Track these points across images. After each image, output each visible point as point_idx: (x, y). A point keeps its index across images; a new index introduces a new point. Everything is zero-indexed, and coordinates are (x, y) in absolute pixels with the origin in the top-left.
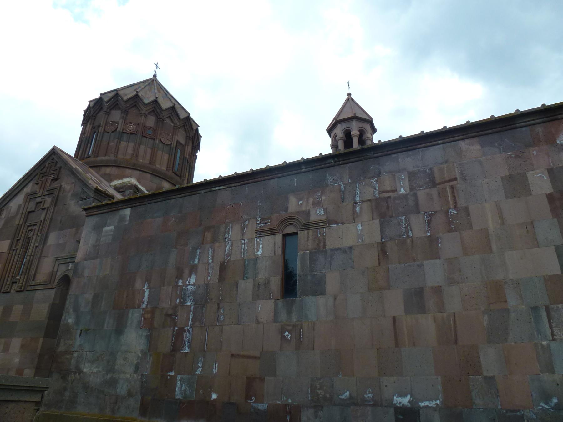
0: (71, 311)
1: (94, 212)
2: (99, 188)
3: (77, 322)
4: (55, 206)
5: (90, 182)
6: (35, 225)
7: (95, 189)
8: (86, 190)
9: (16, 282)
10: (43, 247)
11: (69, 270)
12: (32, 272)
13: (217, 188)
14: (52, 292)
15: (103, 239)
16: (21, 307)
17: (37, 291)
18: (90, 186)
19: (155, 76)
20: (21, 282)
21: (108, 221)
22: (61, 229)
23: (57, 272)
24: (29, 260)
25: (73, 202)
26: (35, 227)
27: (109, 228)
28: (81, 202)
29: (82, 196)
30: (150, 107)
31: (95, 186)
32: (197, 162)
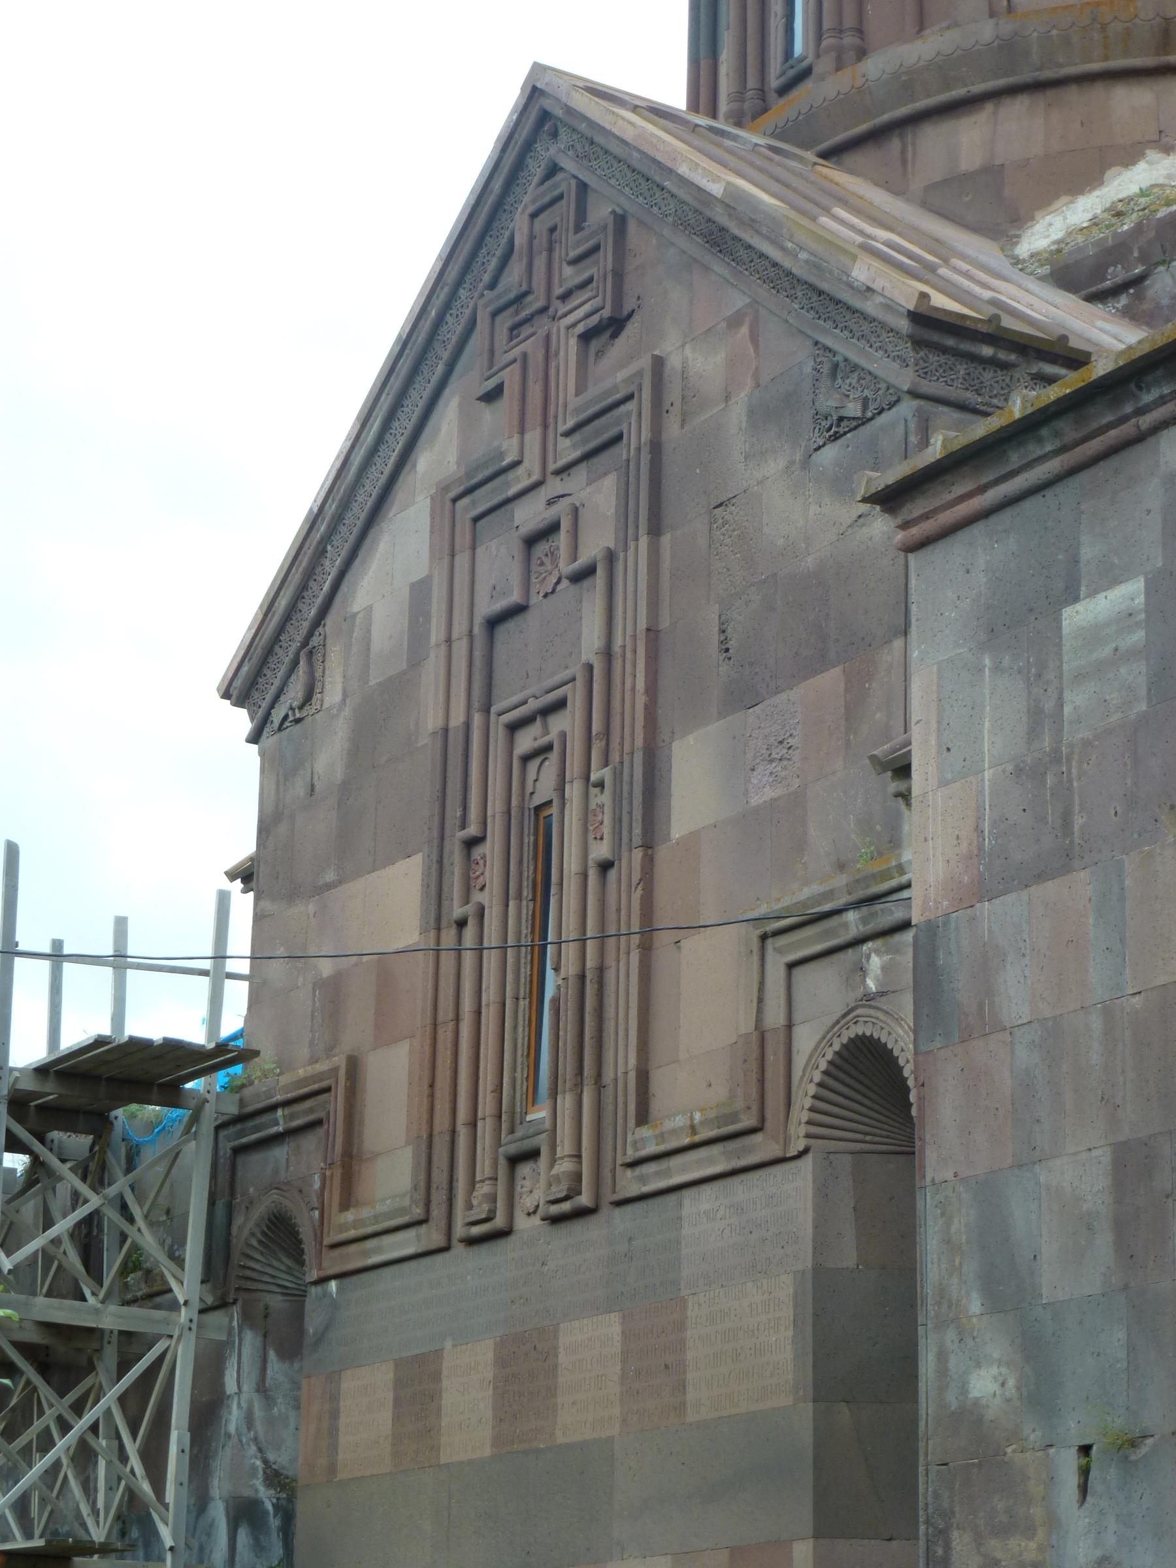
0: (975, 1305)
1: (955, 499)
2: (940, 300)
3: (1040, 1393)
4: (655, 530)
5: (862, 272)
6: (561, 704)
7: (916, 317)
8: (847, 349)
9: (534, 1154)
10: (649, 862)
11: (868, 998)
12: (622, 1060)
14: (796, 1187)
15: (1076, 700)
16: (611, 1327)
17: (686, 1193)
18: (870, 307)
20: (565, 1147)
21: (1088, 551)
22: (742, 696)
23: (789, 1027)
24: (582, 977)
25: (774, 467)
26: (559, 723)
27: (1106, 606)
28: (830, 453)
29: (828, 402)
31: (905, 292)
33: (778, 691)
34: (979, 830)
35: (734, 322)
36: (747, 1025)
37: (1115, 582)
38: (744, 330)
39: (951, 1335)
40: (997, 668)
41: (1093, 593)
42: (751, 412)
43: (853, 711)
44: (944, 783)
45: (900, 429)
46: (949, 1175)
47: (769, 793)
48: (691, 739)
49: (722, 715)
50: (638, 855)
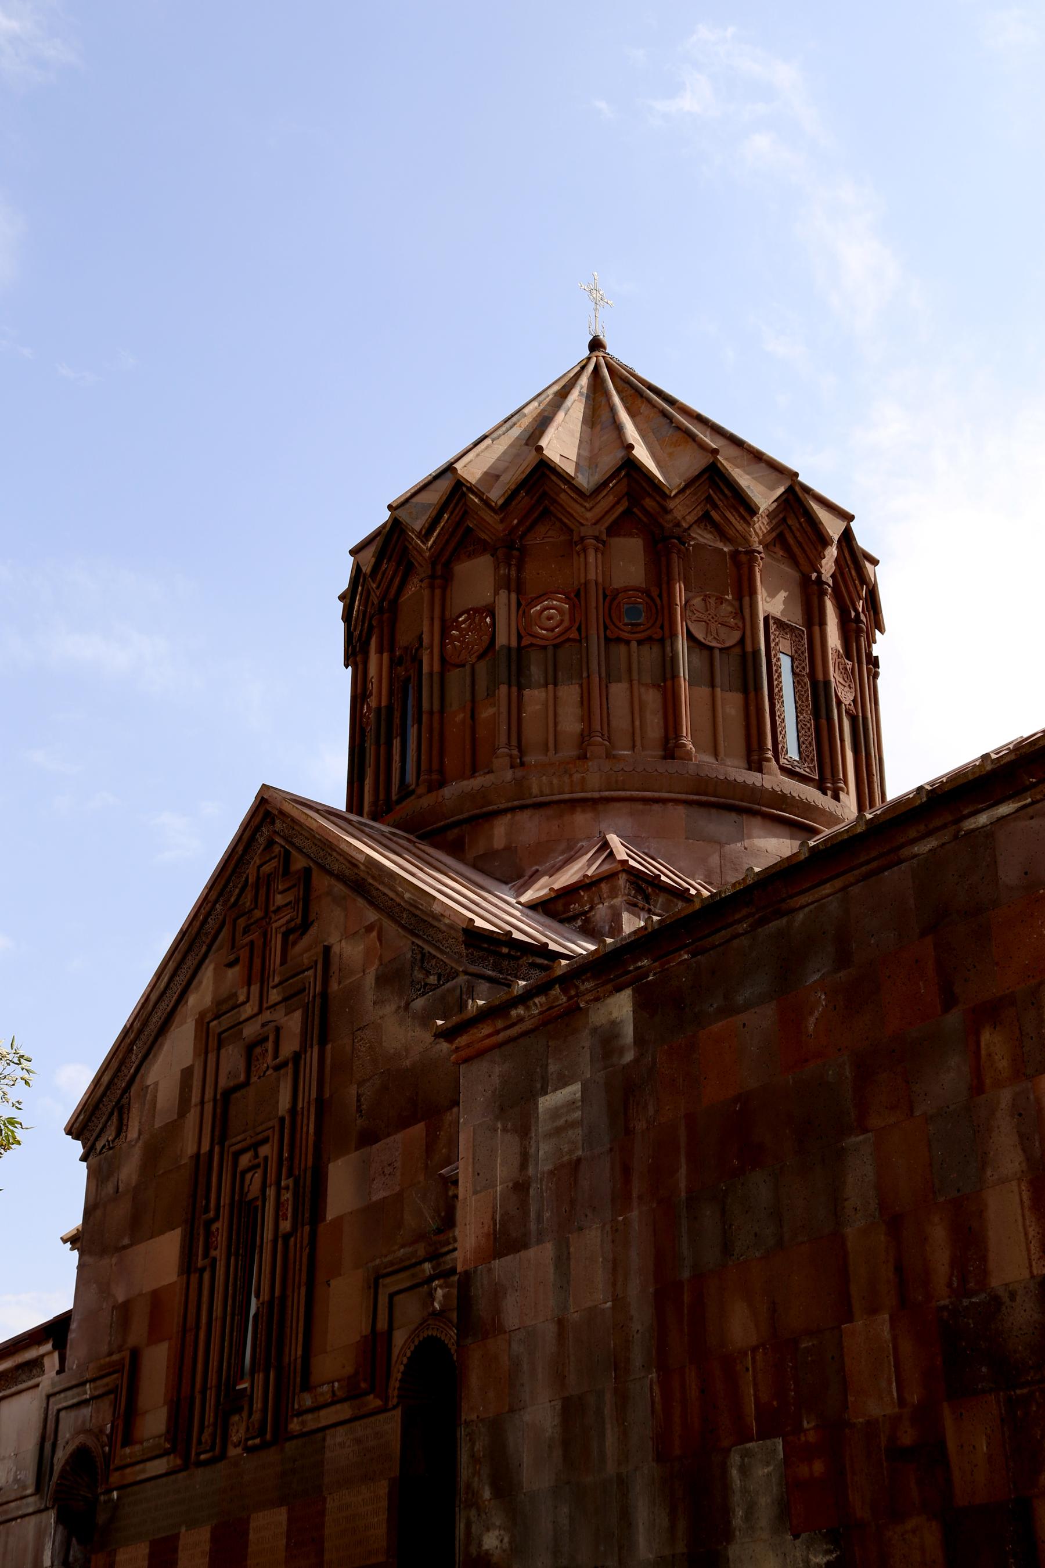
0: (487, 1494)
2: (479, 923)
4: (323, 1042)
7: (465, 931)
11: (434, 1314)
13: (983, 819)
16: (281, 1515)
19: (596, 345)
20: (258, 1405)
21: (553, 1068)
22: (368, 1138)
25: (389, 1009)
26: (264, 1150)
28: (419, 1003)
30: (611, 499)
32: (883, 683)
33: (389, 1135)
34: (494, 1219)
35: (369, 929)
36: (366, 1330)
37: (566, 1085)
38: (374, 934)
39: (473, 1512)
40: (505, 1130)
41: (556, 1090)
42: (378, 979)
43: (430, 1148)
44: (475, 1193)
45: (458, 991)
46: (474, 1417)
47: (382, 1194)
48: (339, 1162)
49: (357, 1149)
50: (307, 1228)
